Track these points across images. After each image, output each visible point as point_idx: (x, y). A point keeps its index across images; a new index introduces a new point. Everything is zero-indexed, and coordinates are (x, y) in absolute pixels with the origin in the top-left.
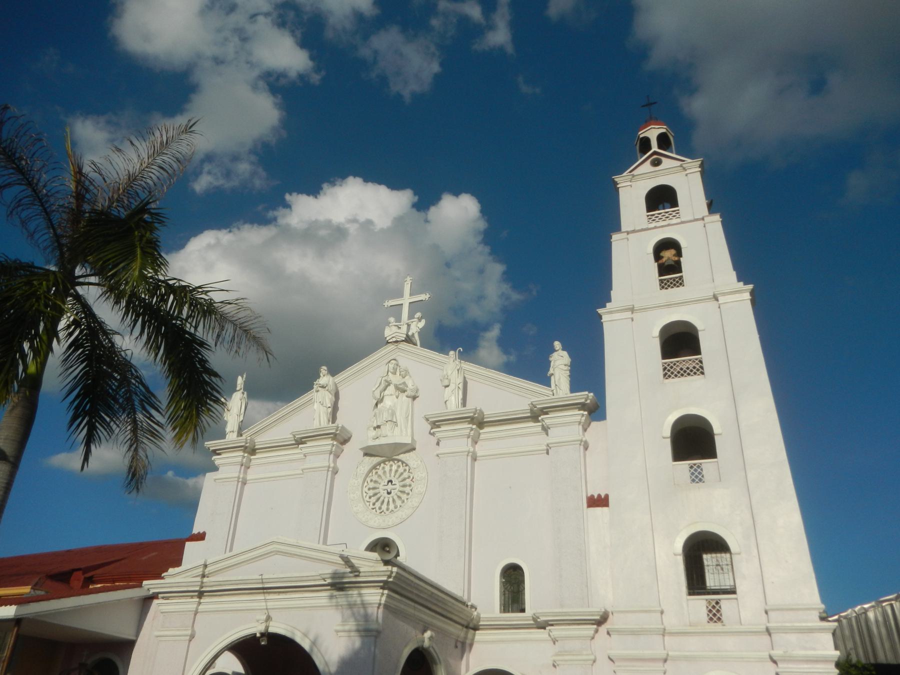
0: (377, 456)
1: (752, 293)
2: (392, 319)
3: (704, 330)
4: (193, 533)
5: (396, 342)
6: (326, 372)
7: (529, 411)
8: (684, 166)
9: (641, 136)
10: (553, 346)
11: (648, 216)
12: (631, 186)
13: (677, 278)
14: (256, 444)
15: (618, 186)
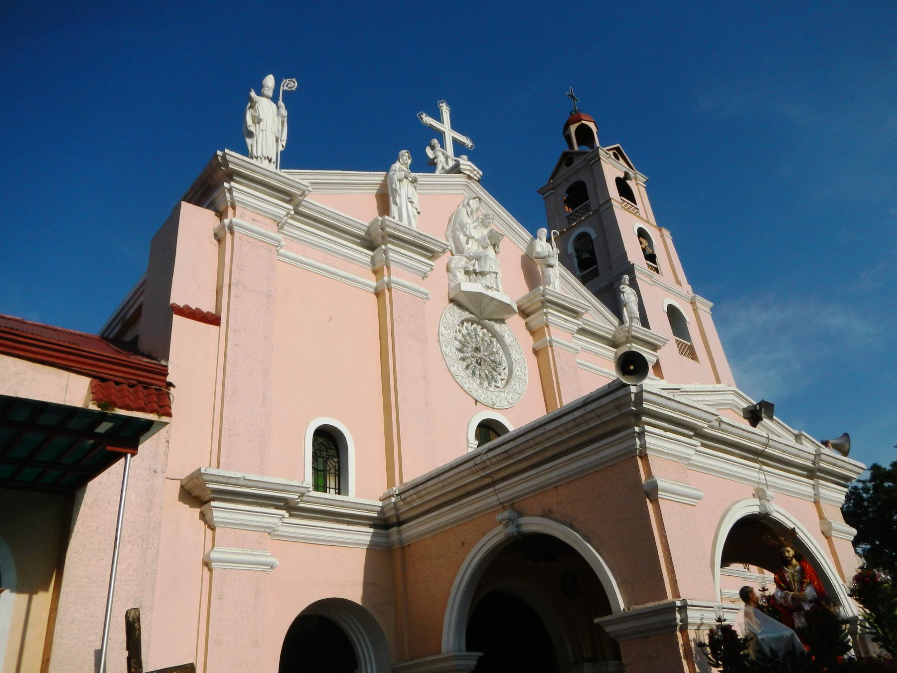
0: (467, 309)
1: (711, 309)
2: (435, 141)
3: (689, 323)
4: (171, 303)
5: (469, 177)
6: (409, 162)
7: (613, 333)
8: (638, 175)
9: (584, 122)
10: (621, 278)
11: (621, 199)
12: (607, 163)
13: (654, 267)
14: (303, 203)
15: (601, 157)
